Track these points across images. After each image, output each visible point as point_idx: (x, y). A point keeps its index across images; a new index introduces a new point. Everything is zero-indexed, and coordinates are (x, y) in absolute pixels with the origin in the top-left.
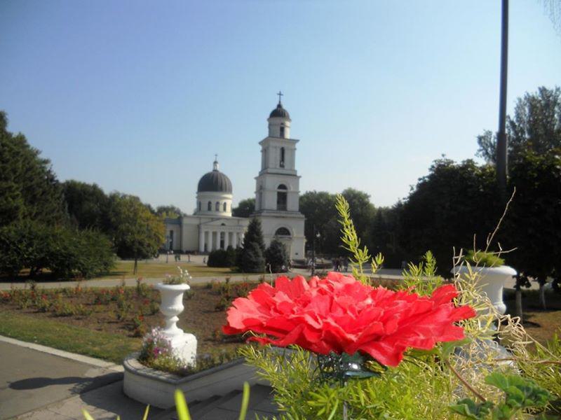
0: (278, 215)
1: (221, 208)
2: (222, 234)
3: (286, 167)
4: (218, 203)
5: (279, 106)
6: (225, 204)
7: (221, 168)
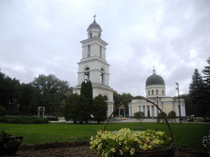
1: (155, 93)
2: (148, 107)
4: (153, 91)
5: (95, 22)
6: (157, 91)
7: (158, 73)
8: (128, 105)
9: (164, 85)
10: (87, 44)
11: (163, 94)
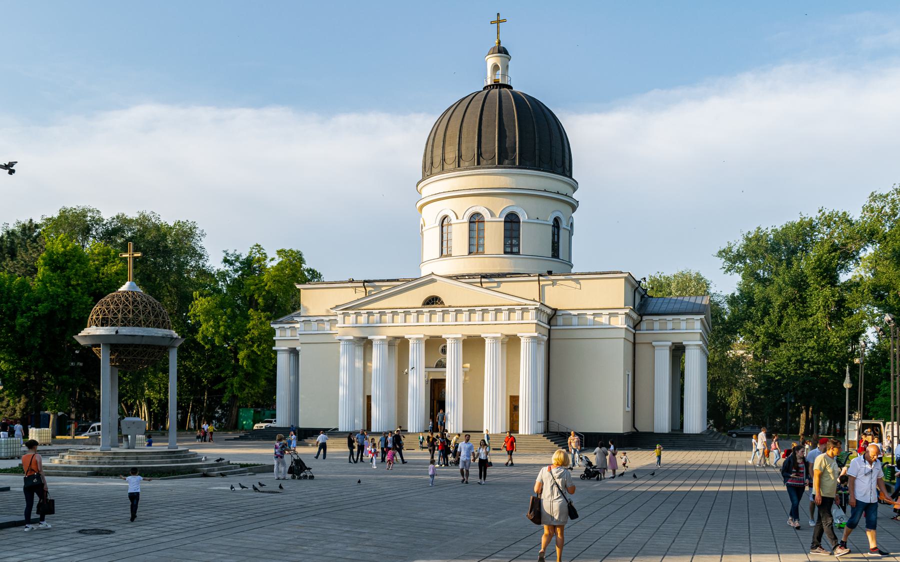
2: (435, 345)
8: (272, 332)
9: (570, 177)
11: (555, 253)
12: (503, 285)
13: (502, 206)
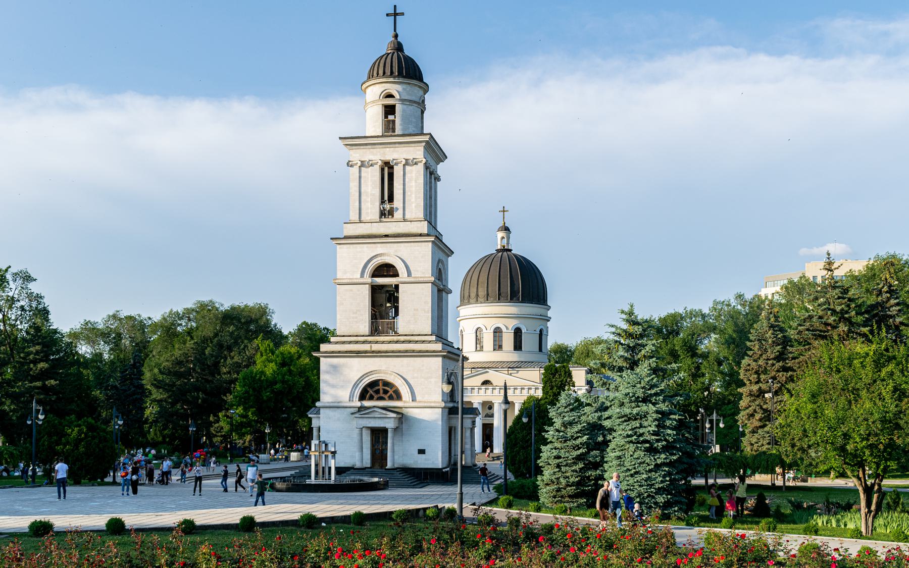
0: (366, 347)
3: (398, 215)
10: (378, 155)
12: (520, 372)
13: (513, 324)
